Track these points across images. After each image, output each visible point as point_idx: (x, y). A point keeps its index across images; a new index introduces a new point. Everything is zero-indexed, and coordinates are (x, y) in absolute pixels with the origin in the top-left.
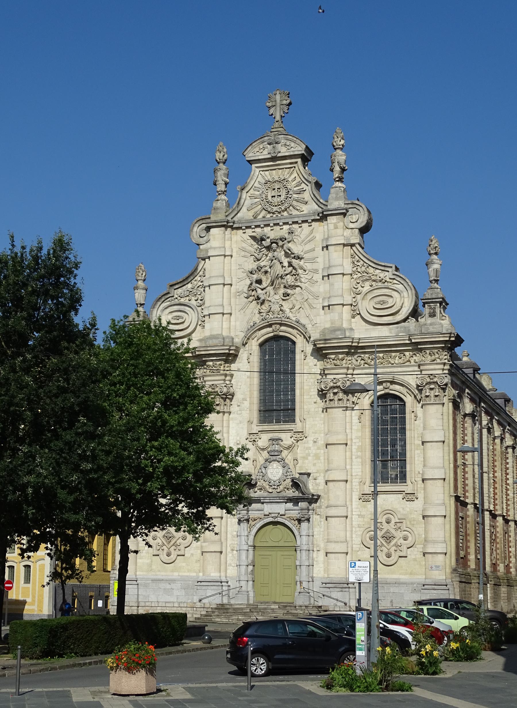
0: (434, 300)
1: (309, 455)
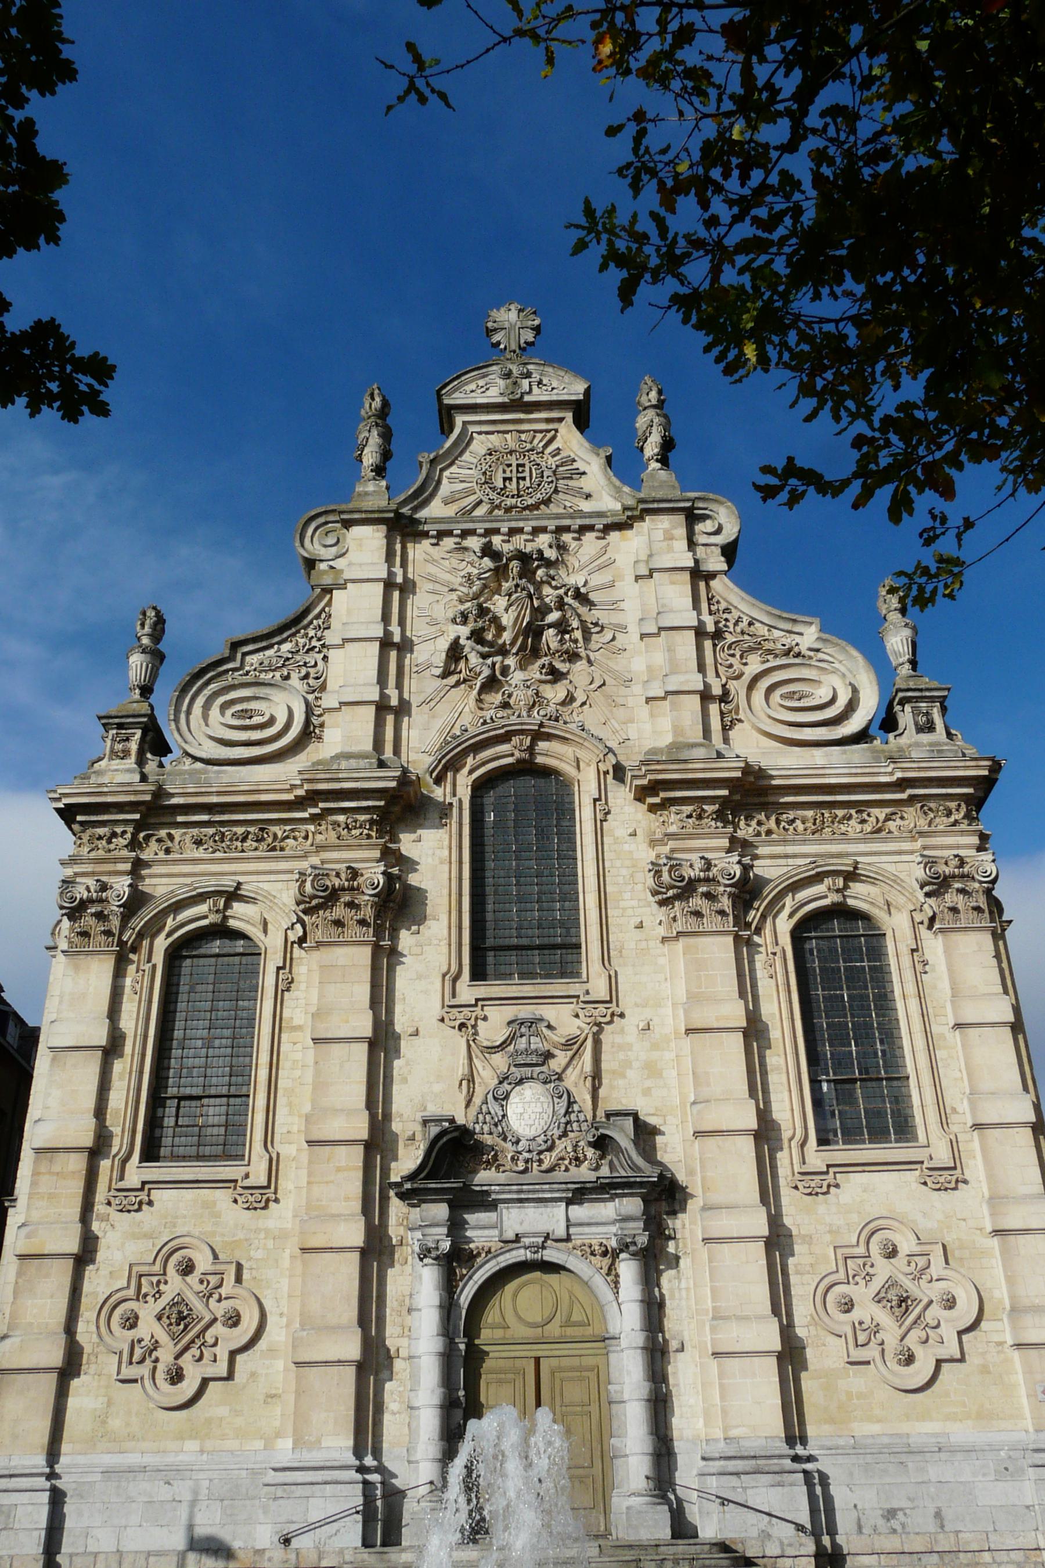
0: (928, 694)
1: (627, 1064)
